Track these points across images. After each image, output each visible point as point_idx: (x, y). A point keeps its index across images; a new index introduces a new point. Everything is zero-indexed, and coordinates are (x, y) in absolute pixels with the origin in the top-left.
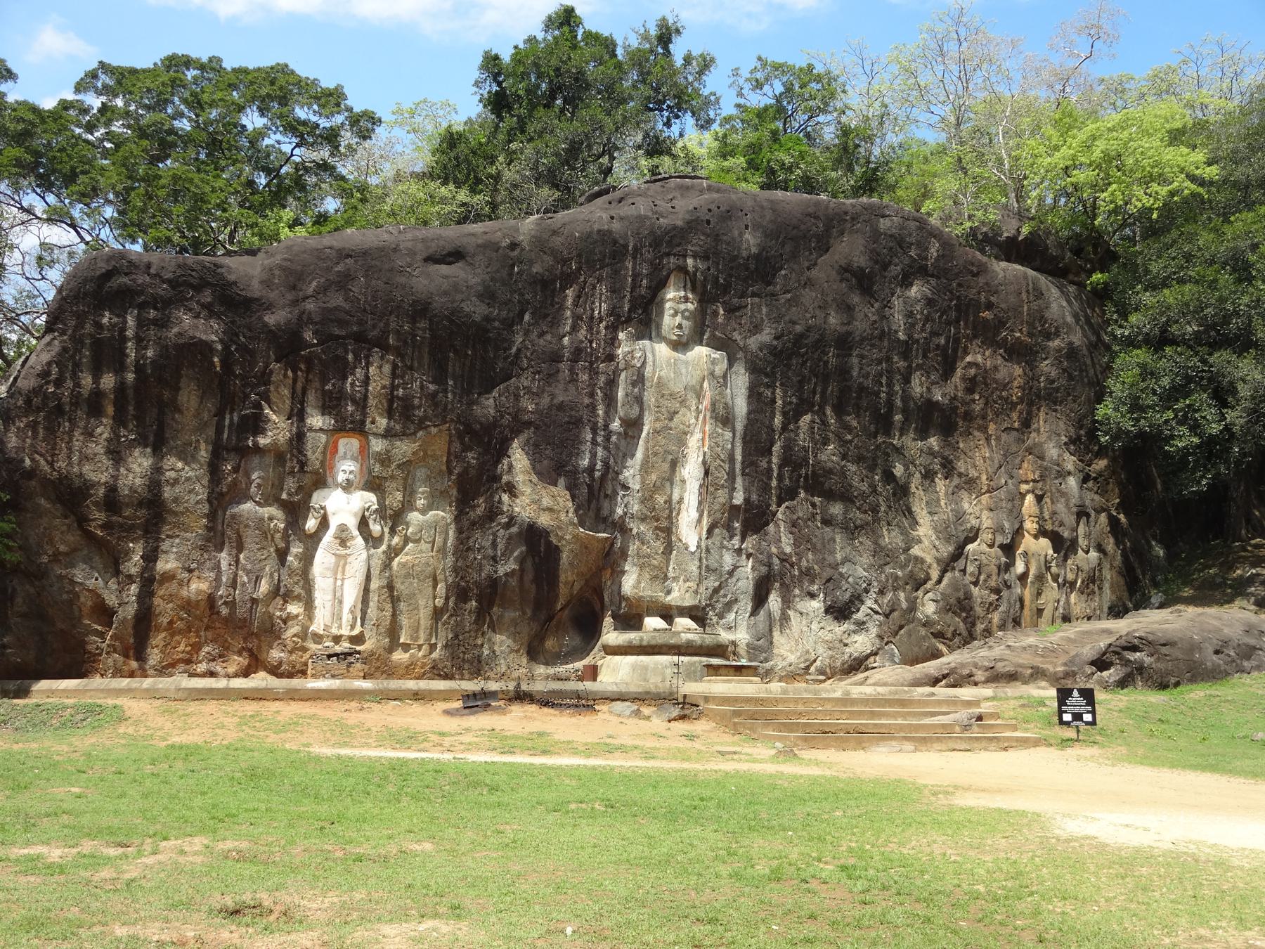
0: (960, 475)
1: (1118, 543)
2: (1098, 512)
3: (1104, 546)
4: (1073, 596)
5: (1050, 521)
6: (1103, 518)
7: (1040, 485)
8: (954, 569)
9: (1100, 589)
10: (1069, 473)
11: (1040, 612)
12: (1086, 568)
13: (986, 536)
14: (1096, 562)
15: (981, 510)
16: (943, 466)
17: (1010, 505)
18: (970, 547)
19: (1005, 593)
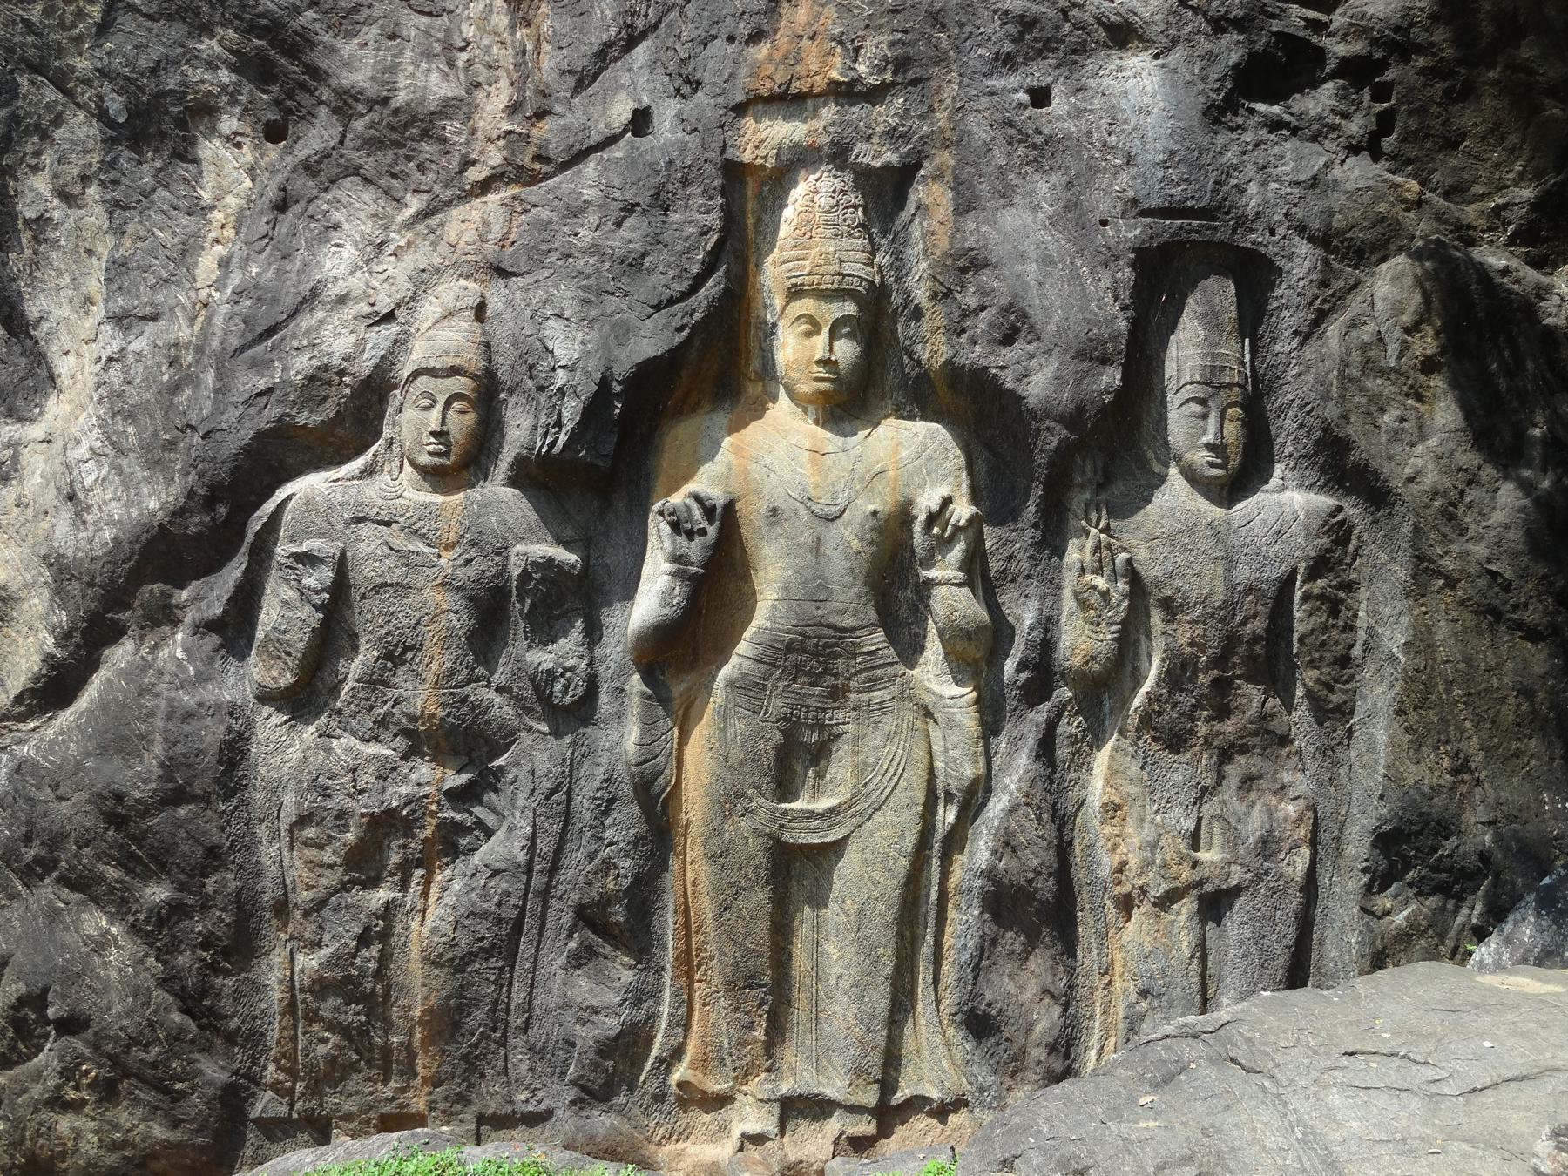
0: (346, 104)
1: (1493, 433)
2: (1349, 250)
3: (1369, 446)
4: (1102, 760)
5: (935, 317)
6: (1390, 286)
7: (885, 114)
8: (164, 616)
9: (1333, 713)
10: (1123, 34)
11: (796, 871)
12: (1203, 582)
13: (414, 421)
14: (1301, 547)
15: (423, 281)
16: (255, 69)
17: (631, 235)
18: (308, 488)
19: (535, 755)
